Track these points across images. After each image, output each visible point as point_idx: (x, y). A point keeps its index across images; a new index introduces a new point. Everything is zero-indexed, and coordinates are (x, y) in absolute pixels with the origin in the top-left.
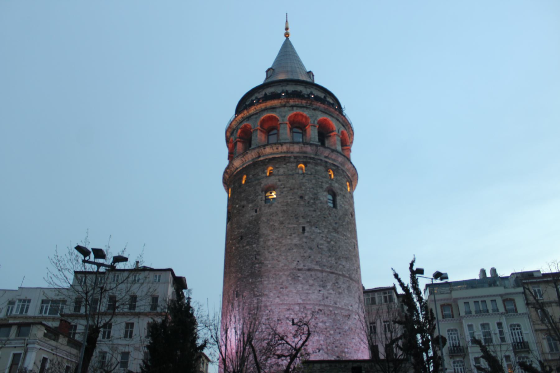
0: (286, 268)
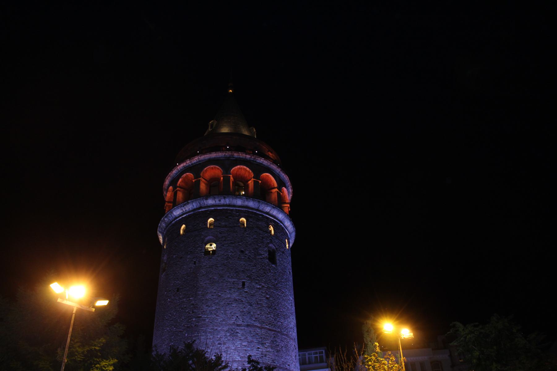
0: (224, 323)
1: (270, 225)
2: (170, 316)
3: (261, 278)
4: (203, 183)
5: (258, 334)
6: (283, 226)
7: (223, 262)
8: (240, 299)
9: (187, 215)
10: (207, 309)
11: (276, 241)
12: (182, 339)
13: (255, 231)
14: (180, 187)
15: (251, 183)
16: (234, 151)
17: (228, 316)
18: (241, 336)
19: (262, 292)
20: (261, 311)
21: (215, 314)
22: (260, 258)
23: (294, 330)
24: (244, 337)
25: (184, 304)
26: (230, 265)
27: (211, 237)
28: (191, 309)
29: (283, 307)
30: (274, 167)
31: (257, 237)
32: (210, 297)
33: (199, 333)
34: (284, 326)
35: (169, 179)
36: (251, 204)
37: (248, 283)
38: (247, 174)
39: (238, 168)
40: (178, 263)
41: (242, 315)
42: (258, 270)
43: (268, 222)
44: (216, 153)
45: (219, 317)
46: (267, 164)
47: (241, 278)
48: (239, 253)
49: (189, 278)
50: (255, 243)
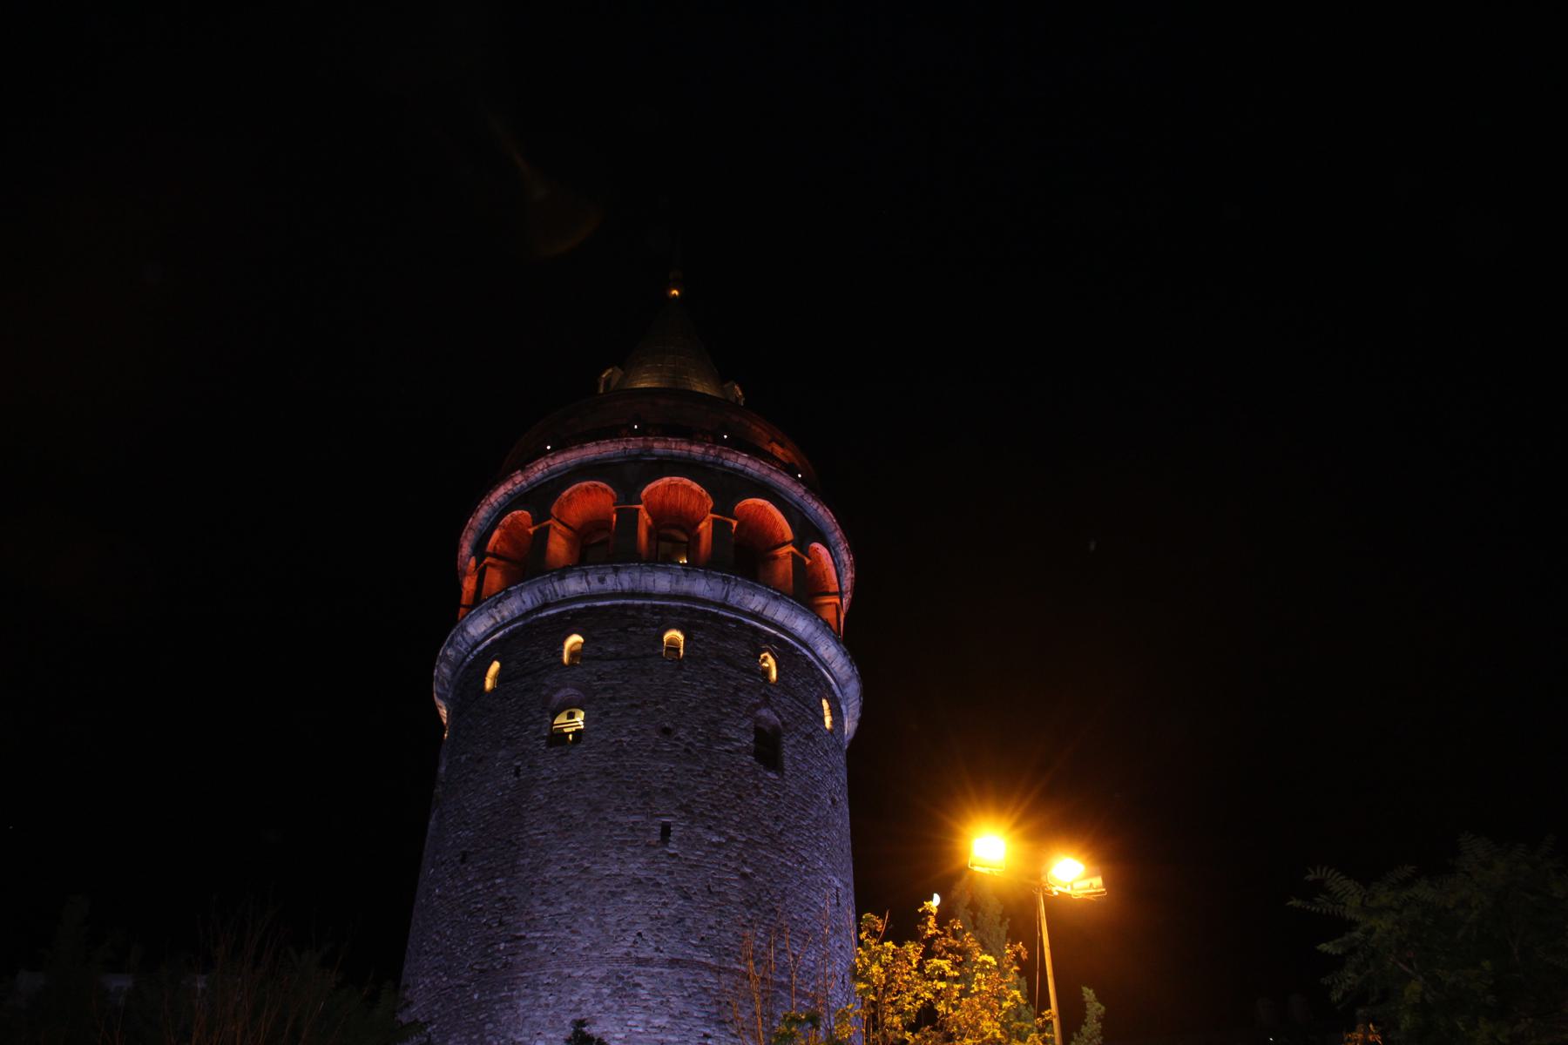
0: (596, 954)
1: (763, 651)
2: (436, 942)
3: (725, 812)
4: (558, 536)
5: (705, 989)
6: (812, 658)
7: (602, 764)
8: (651, 879)
9: (507, 630)
10: (545, 911)
11: (783, 700)
12: (463, 1011)
13: (713, 670)
14: (494, 555)
15: (705, 527)
16: (652, 436)
17: (611, 934)
18: (648, 997)
19: (726, 856)
20: (720, 916)
21: (567, 927)
22: (727, 751)
23: (843, 982)
24: (659, 1000)
25: (477, 900)
26: (626, 774)
27: (571, 692)
28: (497, 913)
29: (802, 907)
30: (782, 481)
31: (717, 685)
32: (555, 875)
33: (514, 990)
34: (805, 969)
35: (469, 538)
36: (701, 587)
37: (681, 829)
38: (694, 504)
39: (665, 486)
40: (471, 776)
41: (654, 928)
42: (716, 788)
43: (758, 641)
44: (597, 444)
45: (580, 934)
46: (758, 471)
47: (658, 813)
48: (657, 737)
49: (497, 817)
50: (710, 705)
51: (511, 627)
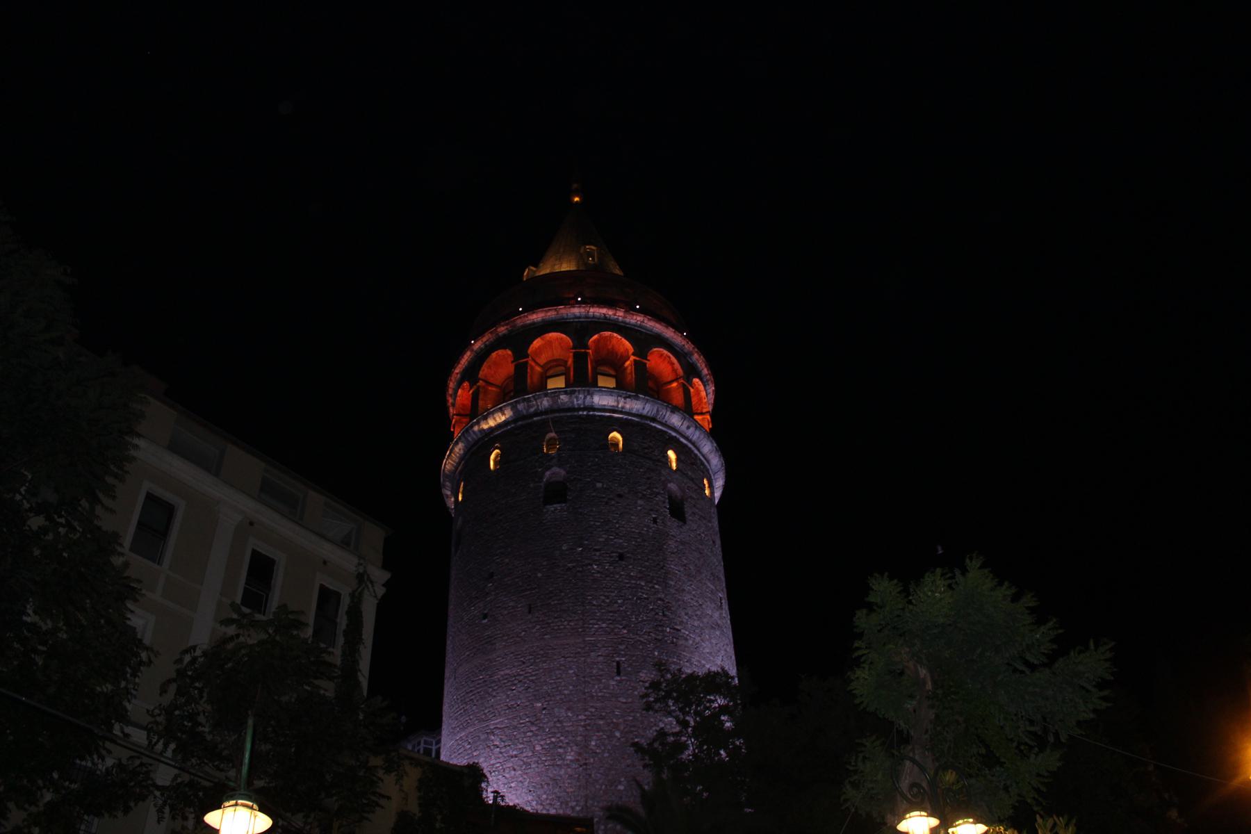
9: (625, 417)
44: (674, 332)
51: (630, 418)
